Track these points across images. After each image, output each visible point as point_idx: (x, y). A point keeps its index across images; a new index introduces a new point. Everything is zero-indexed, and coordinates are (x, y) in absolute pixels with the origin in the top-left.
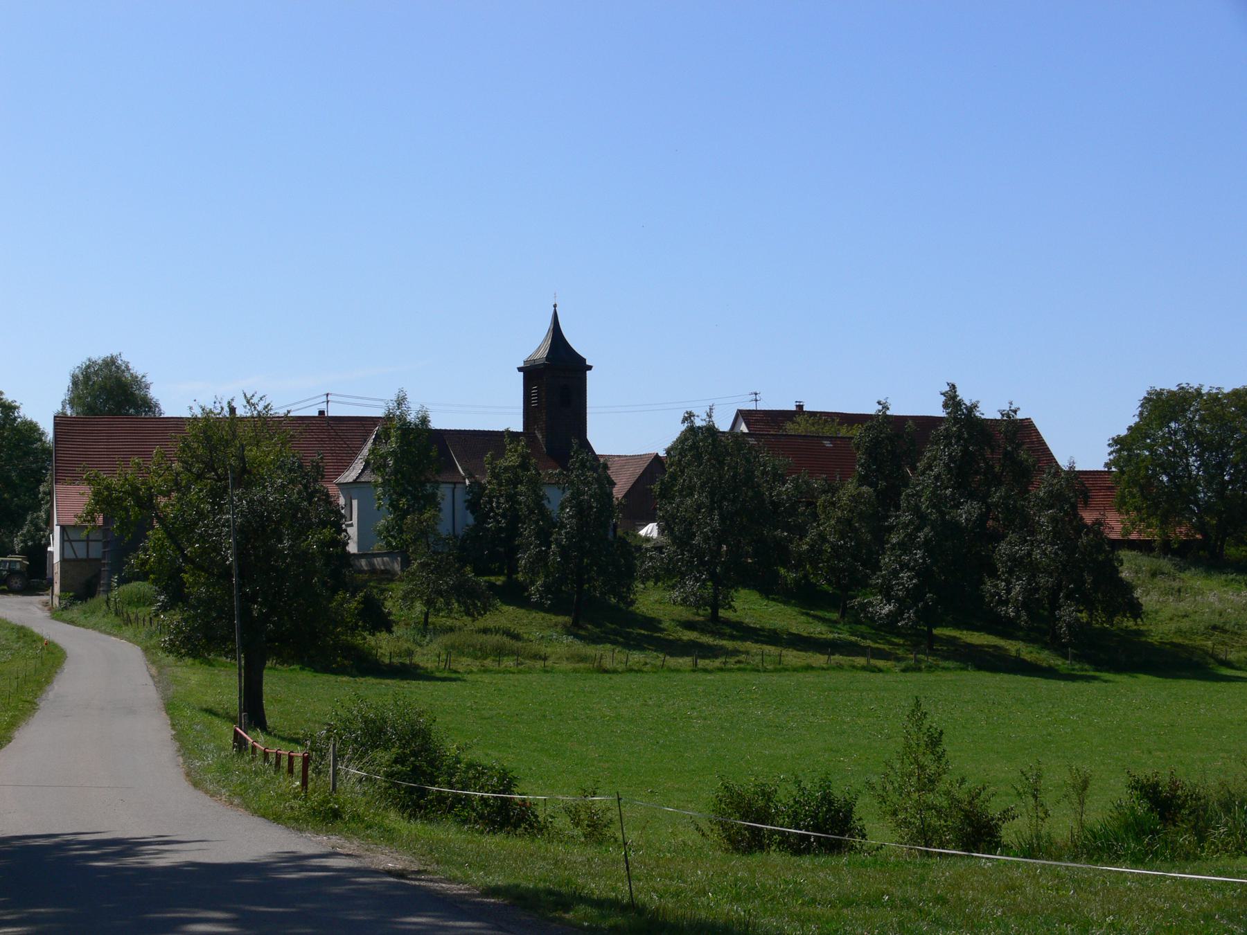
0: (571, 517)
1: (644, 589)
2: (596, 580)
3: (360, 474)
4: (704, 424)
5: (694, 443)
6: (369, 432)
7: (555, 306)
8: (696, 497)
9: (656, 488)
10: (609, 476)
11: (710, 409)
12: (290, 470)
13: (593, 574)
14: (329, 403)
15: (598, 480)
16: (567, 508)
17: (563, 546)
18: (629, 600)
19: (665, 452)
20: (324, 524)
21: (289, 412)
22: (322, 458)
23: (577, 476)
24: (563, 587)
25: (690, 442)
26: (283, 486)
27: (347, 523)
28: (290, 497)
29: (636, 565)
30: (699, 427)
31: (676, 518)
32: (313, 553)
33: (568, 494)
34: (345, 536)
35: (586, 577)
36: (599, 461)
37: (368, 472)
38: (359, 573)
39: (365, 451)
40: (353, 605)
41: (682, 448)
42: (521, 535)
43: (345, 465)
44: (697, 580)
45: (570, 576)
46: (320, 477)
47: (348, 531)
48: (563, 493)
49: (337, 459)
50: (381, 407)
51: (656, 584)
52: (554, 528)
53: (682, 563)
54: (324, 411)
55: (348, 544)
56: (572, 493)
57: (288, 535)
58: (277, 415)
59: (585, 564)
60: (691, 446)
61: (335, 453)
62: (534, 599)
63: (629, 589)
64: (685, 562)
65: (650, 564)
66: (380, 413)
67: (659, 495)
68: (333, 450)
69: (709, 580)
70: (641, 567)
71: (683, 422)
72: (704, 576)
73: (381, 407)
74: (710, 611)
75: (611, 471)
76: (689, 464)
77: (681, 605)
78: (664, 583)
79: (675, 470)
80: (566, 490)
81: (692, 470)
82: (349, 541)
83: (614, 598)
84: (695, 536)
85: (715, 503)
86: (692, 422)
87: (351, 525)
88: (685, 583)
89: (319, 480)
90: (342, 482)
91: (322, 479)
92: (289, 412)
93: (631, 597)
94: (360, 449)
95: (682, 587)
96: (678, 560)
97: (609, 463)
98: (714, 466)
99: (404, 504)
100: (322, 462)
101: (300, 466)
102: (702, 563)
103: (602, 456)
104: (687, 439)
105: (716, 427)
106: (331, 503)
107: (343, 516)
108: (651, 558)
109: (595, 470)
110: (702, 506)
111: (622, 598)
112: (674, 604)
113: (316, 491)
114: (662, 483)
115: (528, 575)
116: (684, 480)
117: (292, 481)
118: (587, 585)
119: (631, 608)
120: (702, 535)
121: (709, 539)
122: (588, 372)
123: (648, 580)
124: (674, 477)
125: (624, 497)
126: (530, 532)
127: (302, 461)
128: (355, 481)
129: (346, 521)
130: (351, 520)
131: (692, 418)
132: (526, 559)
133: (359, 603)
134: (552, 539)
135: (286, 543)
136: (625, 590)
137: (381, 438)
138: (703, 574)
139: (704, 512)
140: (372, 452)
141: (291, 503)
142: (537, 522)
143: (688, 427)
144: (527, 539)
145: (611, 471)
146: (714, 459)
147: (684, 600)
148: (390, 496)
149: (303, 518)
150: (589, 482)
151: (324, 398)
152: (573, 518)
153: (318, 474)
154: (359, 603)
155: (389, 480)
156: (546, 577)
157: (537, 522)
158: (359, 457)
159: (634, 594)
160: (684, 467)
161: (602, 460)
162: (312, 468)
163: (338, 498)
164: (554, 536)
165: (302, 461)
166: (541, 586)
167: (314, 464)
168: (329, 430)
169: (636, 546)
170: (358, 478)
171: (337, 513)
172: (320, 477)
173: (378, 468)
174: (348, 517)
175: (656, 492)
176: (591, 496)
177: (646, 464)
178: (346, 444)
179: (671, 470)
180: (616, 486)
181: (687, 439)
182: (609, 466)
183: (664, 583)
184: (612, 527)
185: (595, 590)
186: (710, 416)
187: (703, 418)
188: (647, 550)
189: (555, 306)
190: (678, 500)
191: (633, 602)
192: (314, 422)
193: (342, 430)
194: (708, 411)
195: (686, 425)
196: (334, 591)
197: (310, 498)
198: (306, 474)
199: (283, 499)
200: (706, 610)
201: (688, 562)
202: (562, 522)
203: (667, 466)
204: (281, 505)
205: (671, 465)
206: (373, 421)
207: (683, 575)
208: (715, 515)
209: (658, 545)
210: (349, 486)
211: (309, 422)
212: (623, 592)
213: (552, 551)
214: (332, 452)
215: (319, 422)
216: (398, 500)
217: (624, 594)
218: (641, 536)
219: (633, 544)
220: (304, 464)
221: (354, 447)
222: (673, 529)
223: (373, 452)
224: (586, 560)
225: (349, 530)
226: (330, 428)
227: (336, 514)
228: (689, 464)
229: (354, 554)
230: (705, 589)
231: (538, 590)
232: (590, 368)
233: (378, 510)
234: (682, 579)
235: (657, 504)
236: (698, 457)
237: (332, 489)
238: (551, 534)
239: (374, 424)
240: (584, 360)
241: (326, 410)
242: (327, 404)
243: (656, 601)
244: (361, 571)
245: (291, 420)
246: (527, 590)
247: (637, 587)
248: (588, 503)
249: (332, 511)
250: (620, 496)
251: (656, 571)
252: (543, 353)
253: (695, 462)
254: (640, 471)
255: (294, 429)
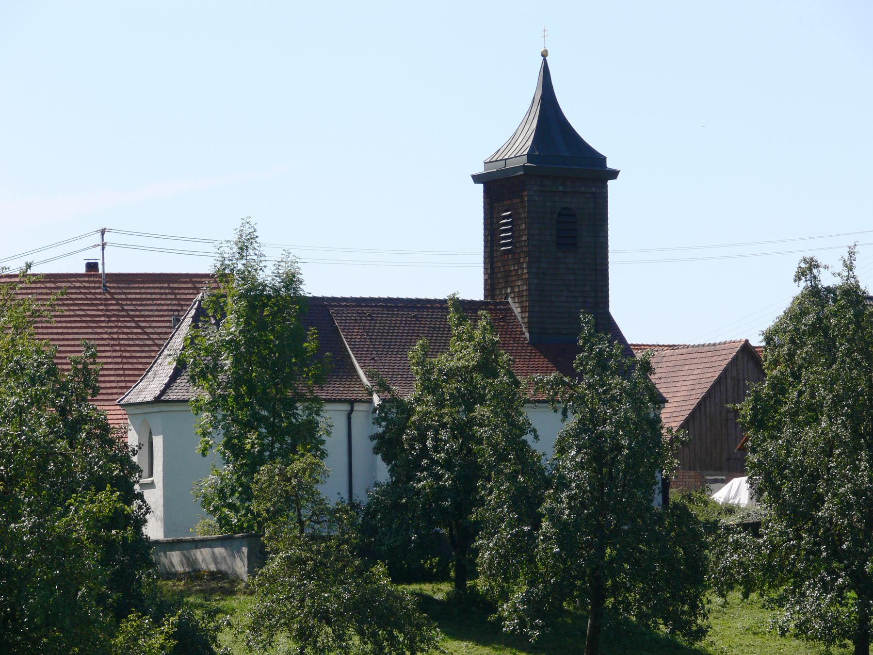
0: (581, 466)
1: (723, 607)
2: (628, 590)
3: (168, 386)
4: (836, 282)
5: (819, 319)
6: (182, 305)
7: (544, 55)
8: (824, 425)
9: (745, 408)
10: (654, 385)
11: (850, 253)
12: (33, 381)
13: (622, 577)
14: (107, 248)
15: (632, 395)
16: (571, 448)
17: (565, 524)
18: (694, 628)
19: (762, 338)
20: (99, 483)
21: (29, 266)
22: (93, 356)
23: (590, 386)
24: (564, 604)
25: (810, 319)
26: (20, 410)
27: (142, 481)
28: (33, 431)
29: (706, 558)
30: (828, 290)
31: (785, 468)
32: (78, 540)
33: (573, 420)
34: (140, 507)
35: (609, 583)
36: (633, 356)
37: (182, 381)
38: (169, 579)
39: (177, 342)
40: (158, 640)
41: (796, 330)
42: (482, 502)
43: (141, 372)
44: (826, 588)
45: (578, 583)
46: (90, 391)
47: (145, 497)
48: (563, 420)
49: (121, 357)
50: (206, 255)
51: (746, 595)
52: (547, 489)
53: (798, 555)
54: (96, 265)
55: (146, 521)
56: (580, 421)
57: (30, 504)
58: (6, 272)
59: (607, 558)
60: (813, 324)
61: (119, 345)
62: (508, 626)
63: (694, 607)
64: (803, 553)
65: (735, 557)
66: (205, 266)
67: (751, 422)
68: (113, 339)
69: (850, 588)
70: (716, 563)
71: (798, 278)
72: (840, 580)
73: (206, 255)
74: (852, 648)
75: (657, 376)
76: (809, 362)
77: (796, 636)
78: (762, 595)
79: (782, 373)
80: (569, 413)
81: (816, 372)
82: (147, 517)
83: (665, 624)
84: (823, 502)
85: (862, 436)
86: (815, 277)
87: (151, 485)
88: (803, 595)
89: (89, 398)
90: (132, 401)
91: (93, 395)
92: (29, 266)
93: (699, 621)
94: (167, 336)
95: (798, 602)
96: (790, 549)
97: (653, 361)
98: (859, 364)
99: (253, 445)
100: (95, 363)
101: (52, 372)
102: (836, 553)
103: (639, 347)
104: (804, 313)
105: (862, 287)
106: (111, 442)
107: (135, 468)
108: (737, 546)
109: (625, 373)
110: (836, 443)
111: (680, 625)
112: (783, 635)
113: (84, 419)
114: (757, 399)
115: (495, 580)
116: (801, 393)
117: (37, 401)
118: (612, 600)
119: (698, 645)
120: (836, 500)
121: (850, 507)
122: (610, 183)
123: (731, 588)
124: (779, 386)
125: (682, 427)
126: (499, 496)
127: (55, 361)
128: (158, 400)
129: (140, 477)
130: (151, 474)
131: (815, 271)
132: (492, 549)
133: (169, 637)
134: (542, 510)
135: (27, 523)
136: (686, 608)
137: (207, 316)
138: (839, 576)
139: (840, 455)
140: (191, 342)
141: (36, 443)
142: (512, 477)
143: (806, 289)
144: (494, 509)
145: (657, 376)
146: (860, 351)
147: (802, 629)
148: (227, 428)
149: (58, 471)
150: (613, 398)
151: (97, 239)
152: (582, 468)
153: (87, 386)
154: (169, 637)
155: (224, 398)
156: (532, 583)
157: (512, 477)
158: (166, 352)
159: (705, 616)
160: (800, 367)
161: (639, 355)
162: (75, 375)
163: (125, 432)
164: (547, 504)
165: (55, 361)
166: (523, 602)
167: (80, 366)
168: (106, 299)
169: (708, 522)
170: (163, 392)
171: (125, 461)
172: (90, 391)
173: (203, 375)
174: (146, 472)
175: (744, 417)
176: (619, 425)
177: (727, 362)
178: (139, 327)
179: (774, 373)
180: (667, 405)
181: (804, 313)
182: (654, 365)
183: (762, 595)
184: (660, 485)
185: (627, 609)
186: (850, 268)
187: (837, 272)
188: (728, 529)
189: (544, 55)
190: (787, 431)
191: (702, 632)
192: (78, 285)
193: (131, 299)
194: (846, 256)
195: (803, 284)
196: (121, 614)
197: (72, 431)
198: (64, 387)
199: (19, 436)
200: (845, 646)
201: (809, 552)
202: (563, 477)
203: (766, 364)
204: (16, 447)
205: (775, 363)
206: (194, 280)
207: (799, 579)
208: (860, 460)
209: (750, 520)
210: (141, 410)
211: (68, 285)
212: (683, 613)
213: (544, 535)
214: (112, 342)
215: (87, 285)
216: (242, 437)
217: (685, 617)
218: (715, 503)
219: (702, 519)
220: (60, 367)
221: (156, 333)
222: (779, 489)
223: (192, 342)
224: (608, 551)
225: (148, 494)
226: (108, 296)
227: (122, 465)
228: (809, 362)
229: (157, 542)
230: (842, 605)
231: (516, 610)
232: (614, 174)
233: (204, 454)
234: (797, 585)
235: (747, 440)
236: (828, 348)
237: (114, 416)
238: (542, 500)
239: (194, 288)
240: (603, 159)
241: (100, 263)
242: (103, 249)
243: (748, 629)
244: (171, 575)
245: (34, 282)
246: (495, 611)
247: (709, 602)
248: (613, 438)
249: (113, 459)
250: (675, 425)
251: (745, 570)
252: (524, 144)
253: (819, 356)
254: (714, 375)
255: (38, 300)
